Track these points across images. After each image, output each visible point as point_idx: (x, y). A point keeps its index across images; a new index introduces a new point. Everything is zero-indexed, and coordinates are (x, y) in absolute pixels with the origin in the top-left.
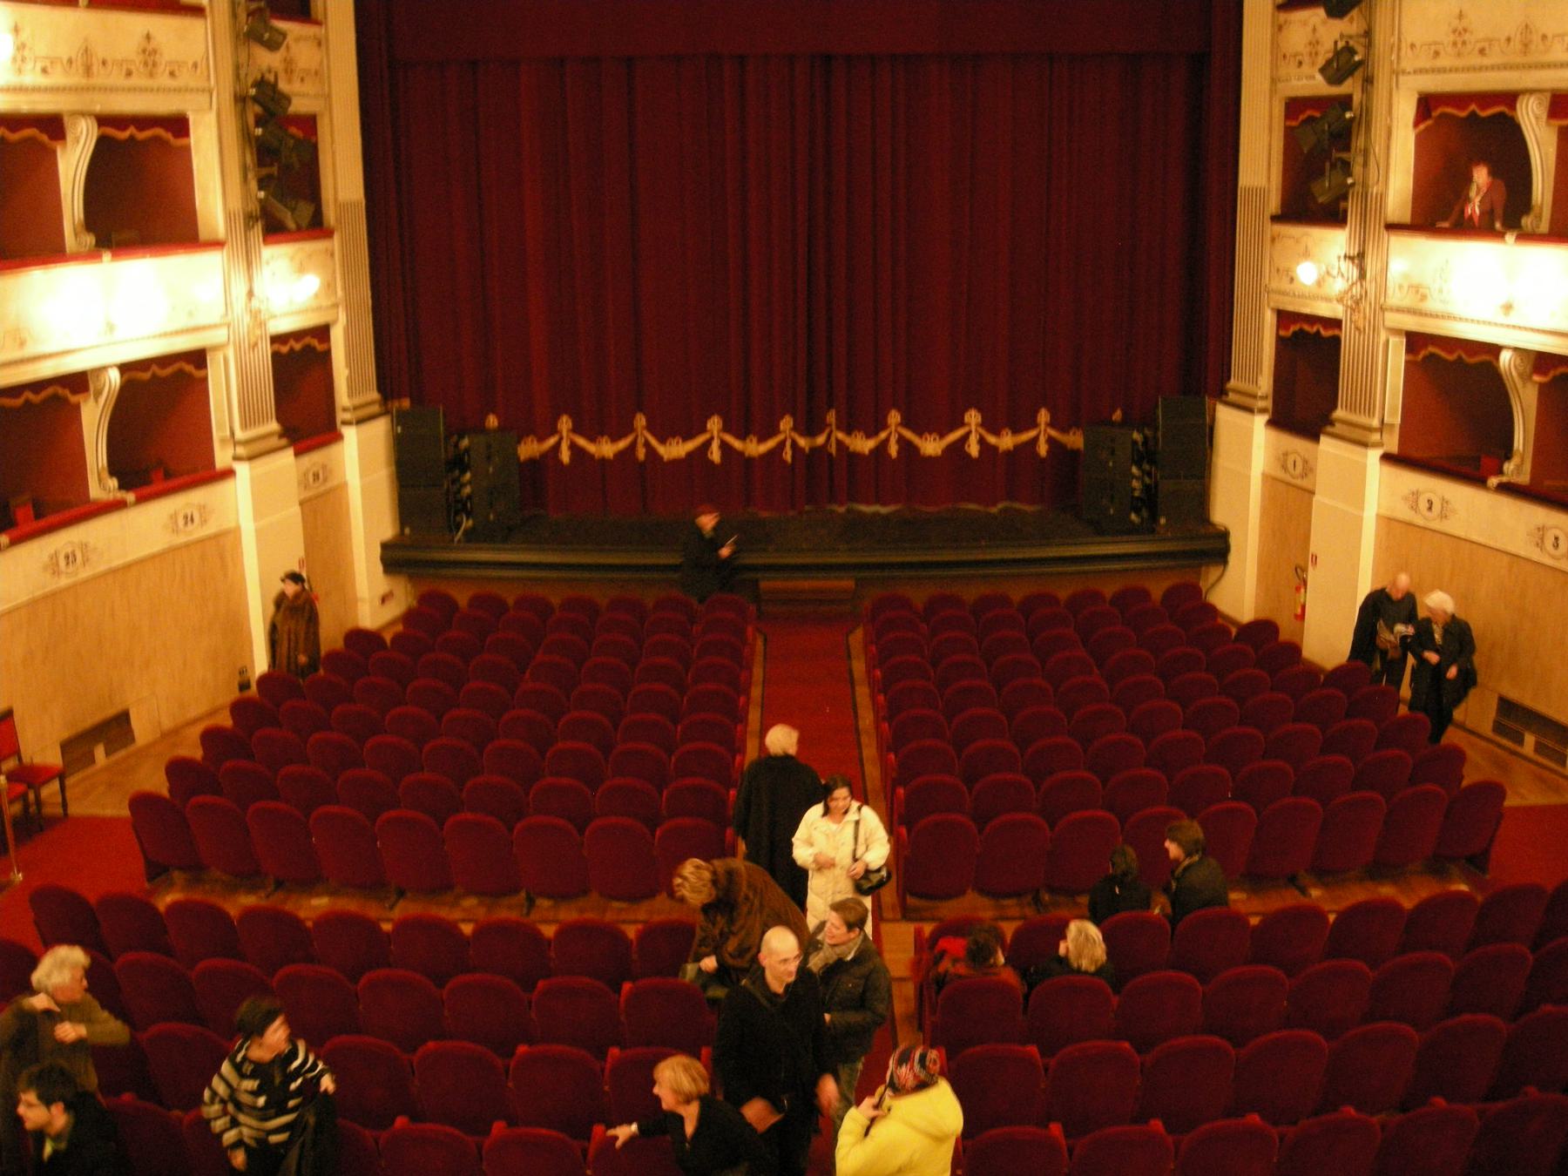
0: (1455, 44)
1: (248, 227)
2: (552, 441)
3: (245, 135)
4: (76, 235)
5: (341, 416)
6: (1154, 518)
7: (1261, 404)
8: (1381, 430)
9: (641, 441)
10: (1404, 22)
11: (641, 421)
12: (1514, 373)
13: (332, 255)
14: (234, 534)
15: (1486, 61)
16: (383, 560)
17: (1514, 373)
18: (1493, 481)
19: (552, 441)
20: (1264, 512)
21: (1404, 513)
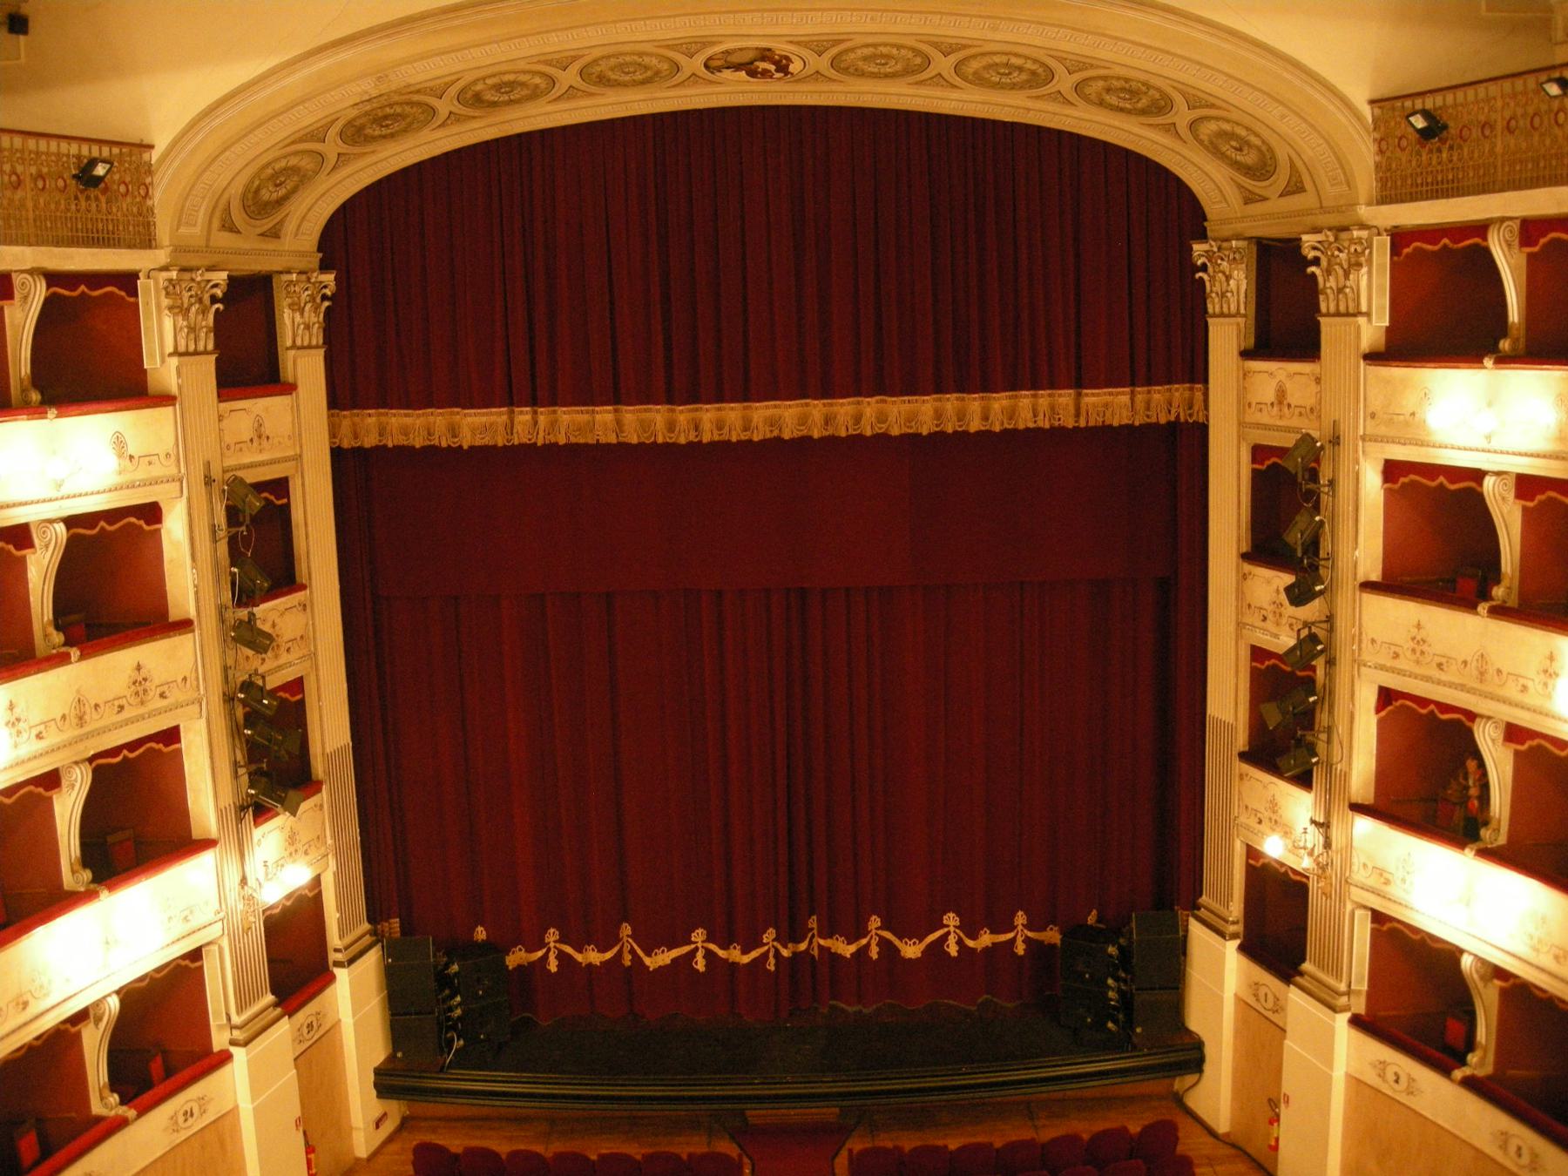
1: (240, 820)
2: (540, 953)
3: (235, 731)
4: (73, 872)
5: (333, 956)
6: (1130, 1024)
7: (1232, 929)
8: (1348, 993)
9: (627, 948)
10: (1365, 618)
11: (626, 930)
12: (1475, 976)
13: (322, 806)
14: (234, 1112)
15: (1444, 677)
16: (376, 1085)
17: (1475, 976)
18: (1458, 1074)
19: (540, 953)
20: (1238, 1033)
21: (1371, 1077)
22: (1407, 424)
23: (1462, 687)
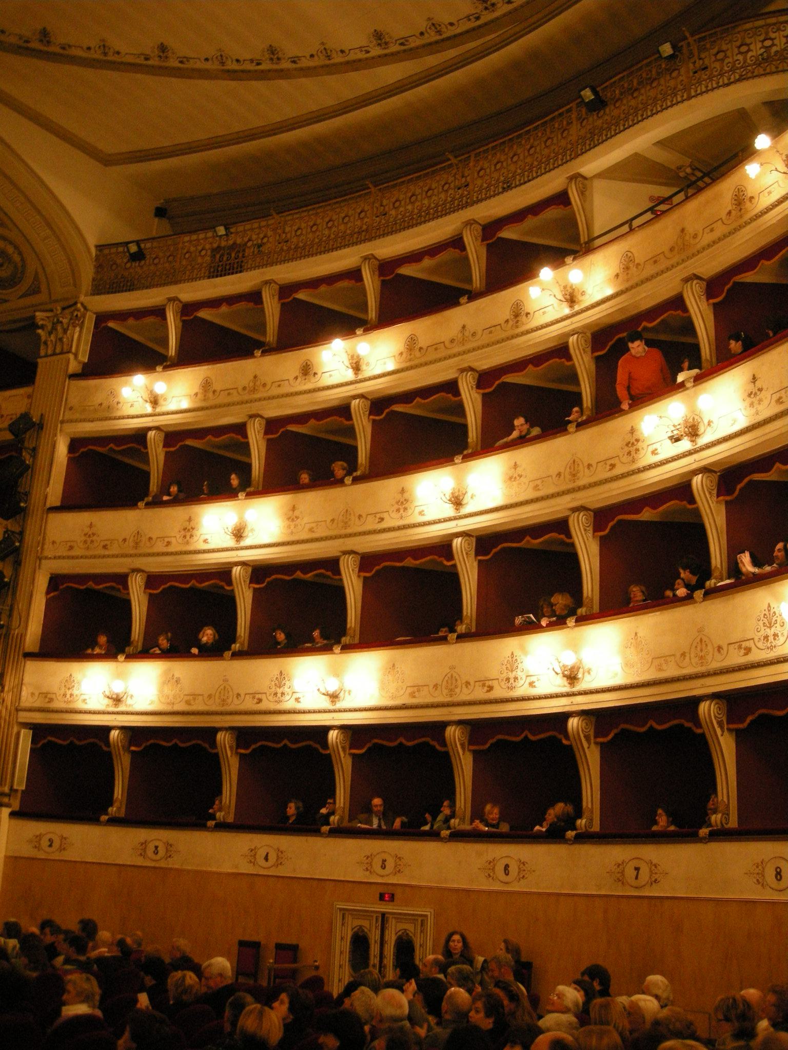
0: (85, 542)
15: (107, 553)
22: (96, 410)
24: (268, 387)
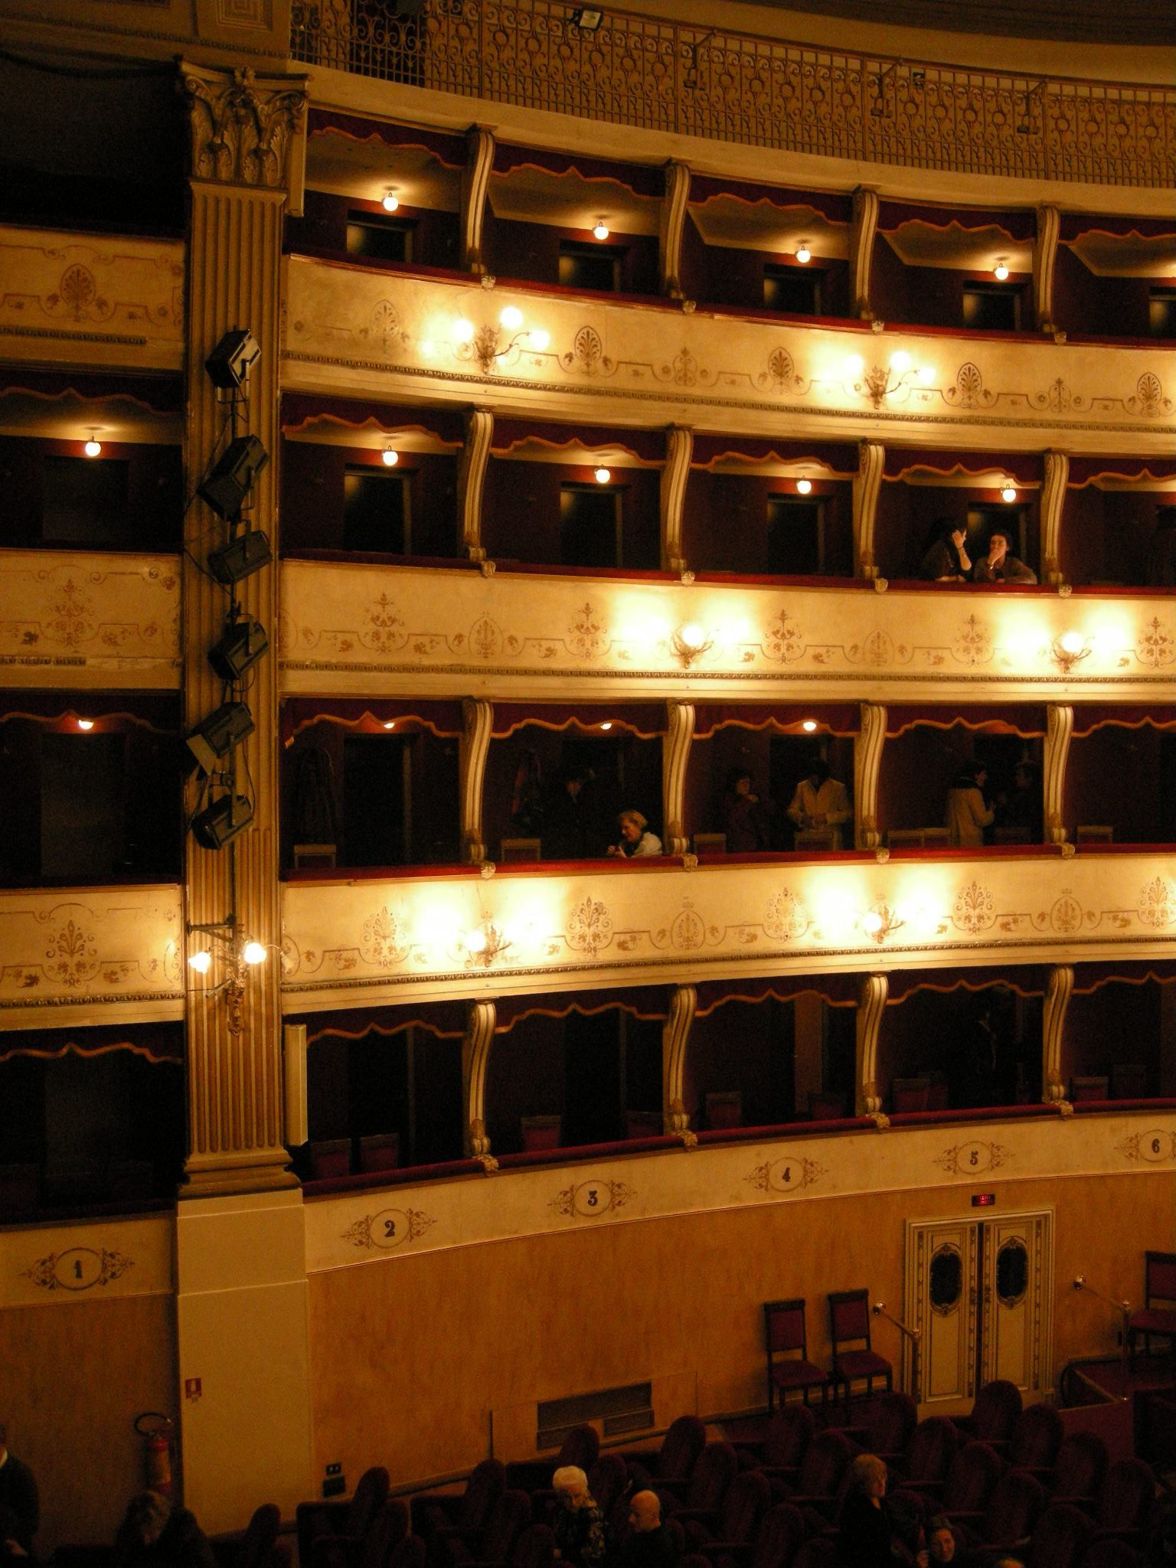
0: (376, 636)
15: (426, 661)
22: (354, 343)
23: (461, 670)
24: (713, 379)
